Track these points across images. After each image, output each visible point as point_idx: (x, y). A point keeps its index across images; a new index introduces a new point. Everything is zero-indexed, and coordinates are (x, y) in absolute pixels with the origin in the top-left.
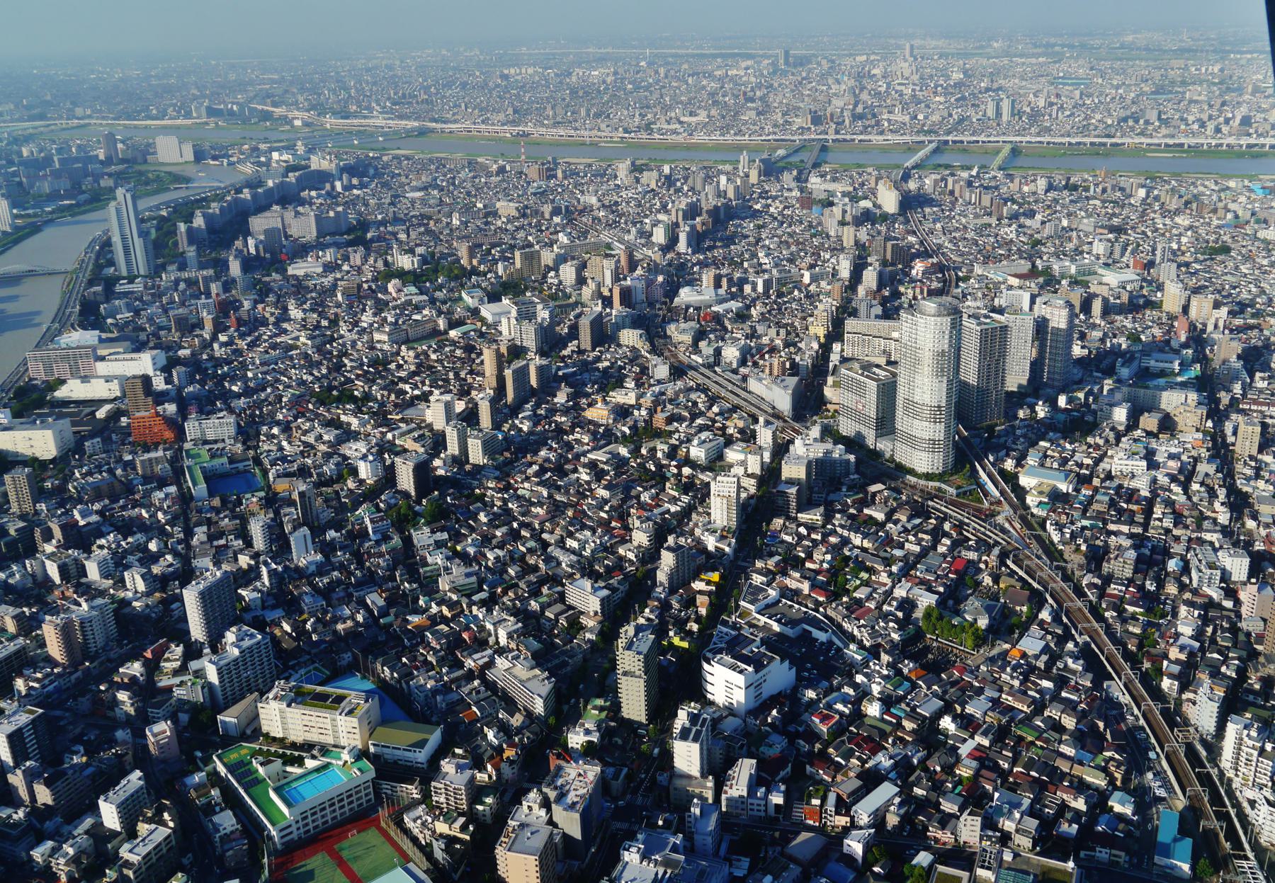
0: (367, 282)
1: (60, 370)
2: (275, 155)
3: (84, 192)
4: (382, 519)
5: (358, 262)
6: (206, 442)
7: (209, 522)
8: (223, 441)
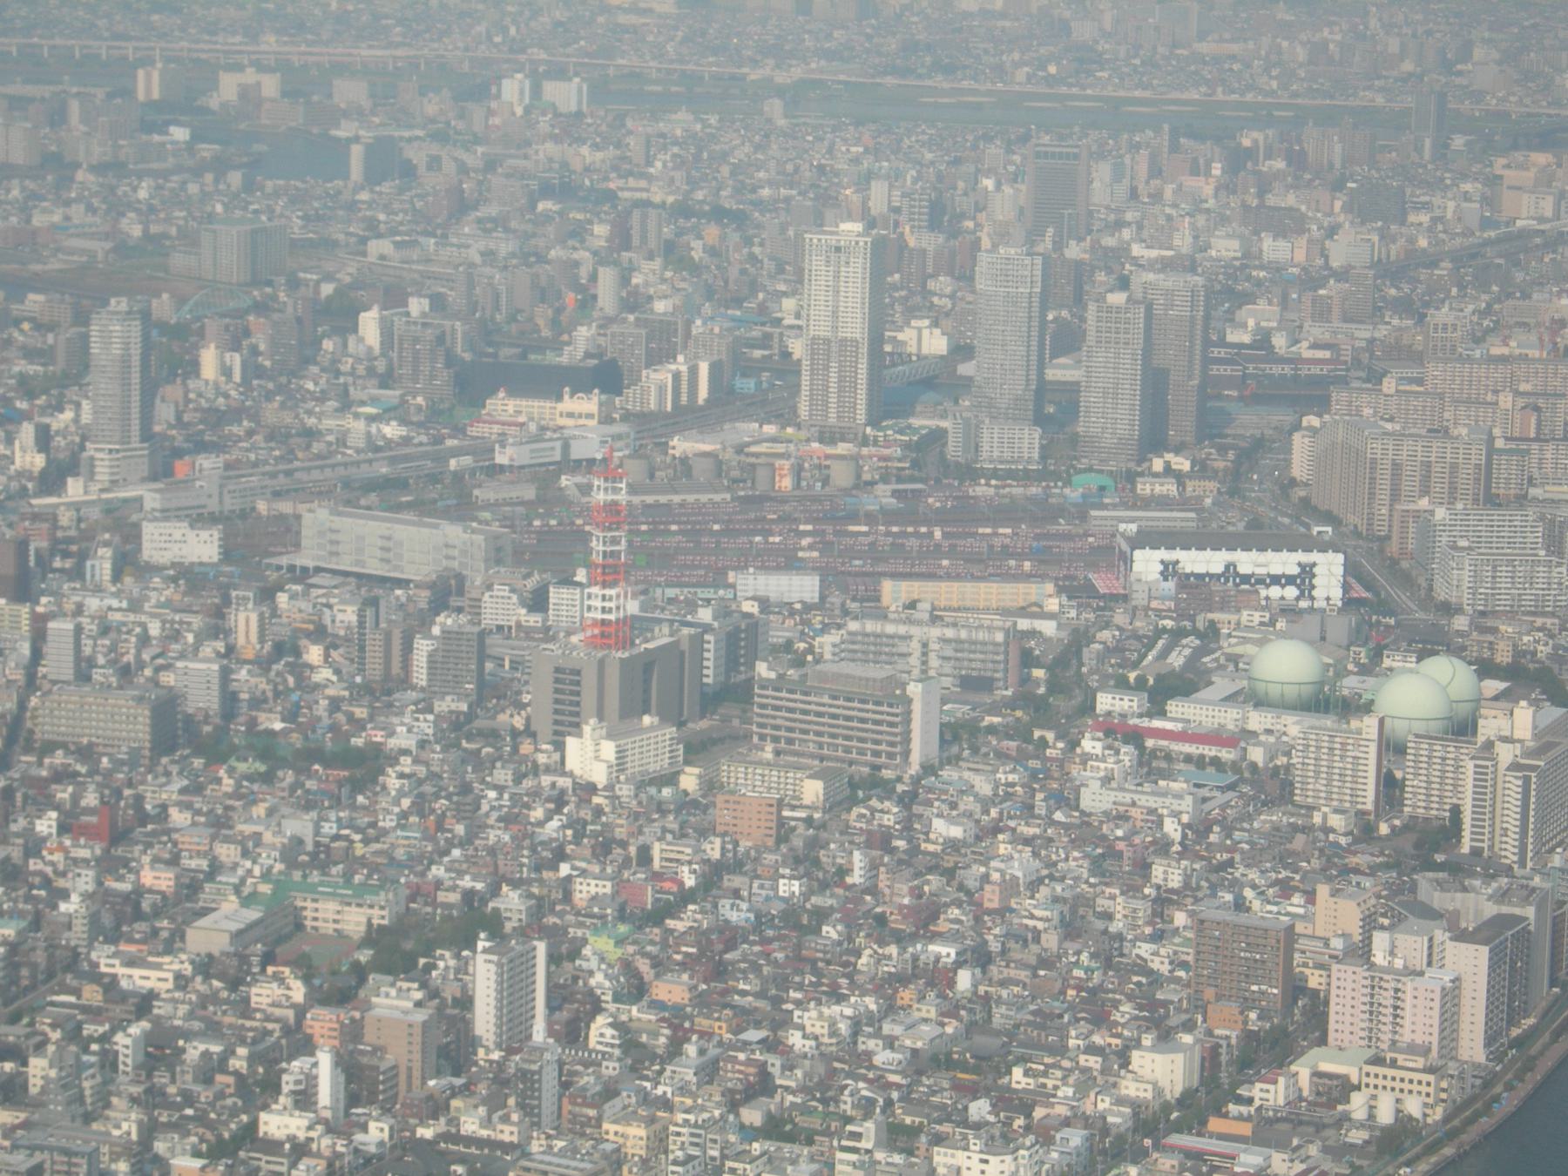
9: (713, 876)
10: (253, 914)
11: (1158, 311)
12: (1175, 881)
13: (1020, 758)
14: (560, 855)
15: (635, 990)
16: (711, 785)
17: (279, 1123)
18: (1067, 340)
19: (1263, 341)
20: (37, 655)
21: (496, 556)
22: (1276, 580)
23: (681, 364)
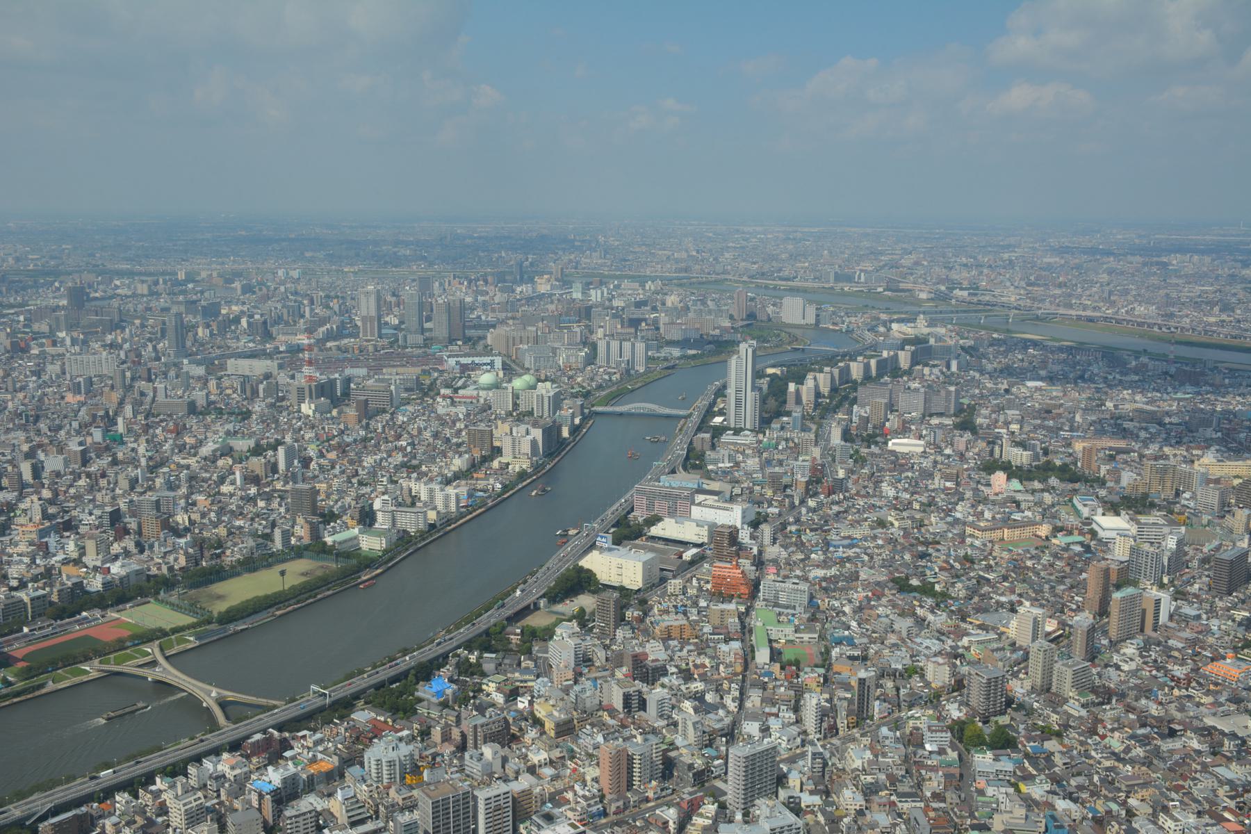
0: (967, 470)
1: (660, 507)
2: (895, 326)
4: (942, 731)
5: (962, 447)
6: (776, 605)
7: (764, 687)
8: (794, 608)
9: (342, 432)
10: (217, 446)
12: (463, 426)
14: (300, 429)
15: (321, 455)
16: (340, 413)
17: (225, 489)
18: (429, 319)
19: (479, 317)
21: (281, 367)
22: (485, 364)
23: (328, 326)
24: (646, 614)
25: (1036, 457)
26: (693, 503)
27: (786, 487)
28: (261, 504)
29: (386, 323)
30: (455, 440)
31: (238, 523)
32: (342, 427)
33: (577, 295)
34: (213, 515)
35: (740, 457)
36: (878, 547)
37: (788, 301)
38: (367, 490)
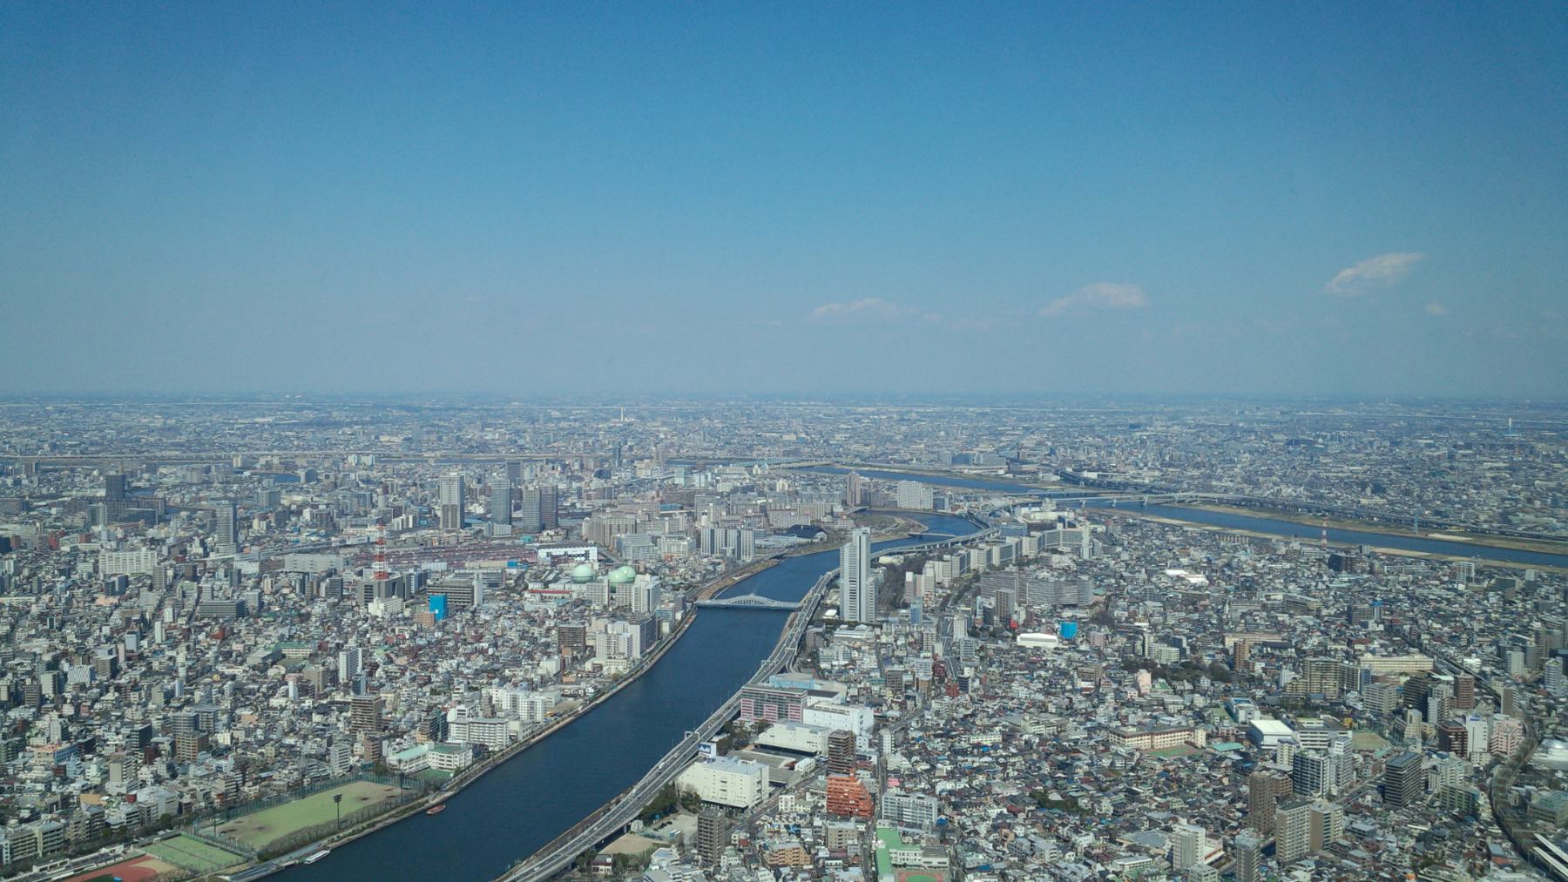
3: (822, 530)
5: (1099, 642)
6: (901, 822)
9: (414, 635)
11: (543, 493)
12: (552, 625)
13: (505, 601)
14: (367, 632)
15: (391, 661)
16: (413, 613)
17: (274, 702)
18: (518, 508)
19: (573, 505)
20: (199, 597)
23: (404, 517)
24: (753, 837)
25: (1182, 651)
26: (805, 706)
27: (907, 687)
28: (316, 718)
29: (469, 513)
30: (543, 640)
31: (290, 741)
32: (415, 628)
33: (680, 481)
34: (259, 732)
35: (855, 654)
36: (1014, 755)
37: (903, 485)
38: (442, 698)
